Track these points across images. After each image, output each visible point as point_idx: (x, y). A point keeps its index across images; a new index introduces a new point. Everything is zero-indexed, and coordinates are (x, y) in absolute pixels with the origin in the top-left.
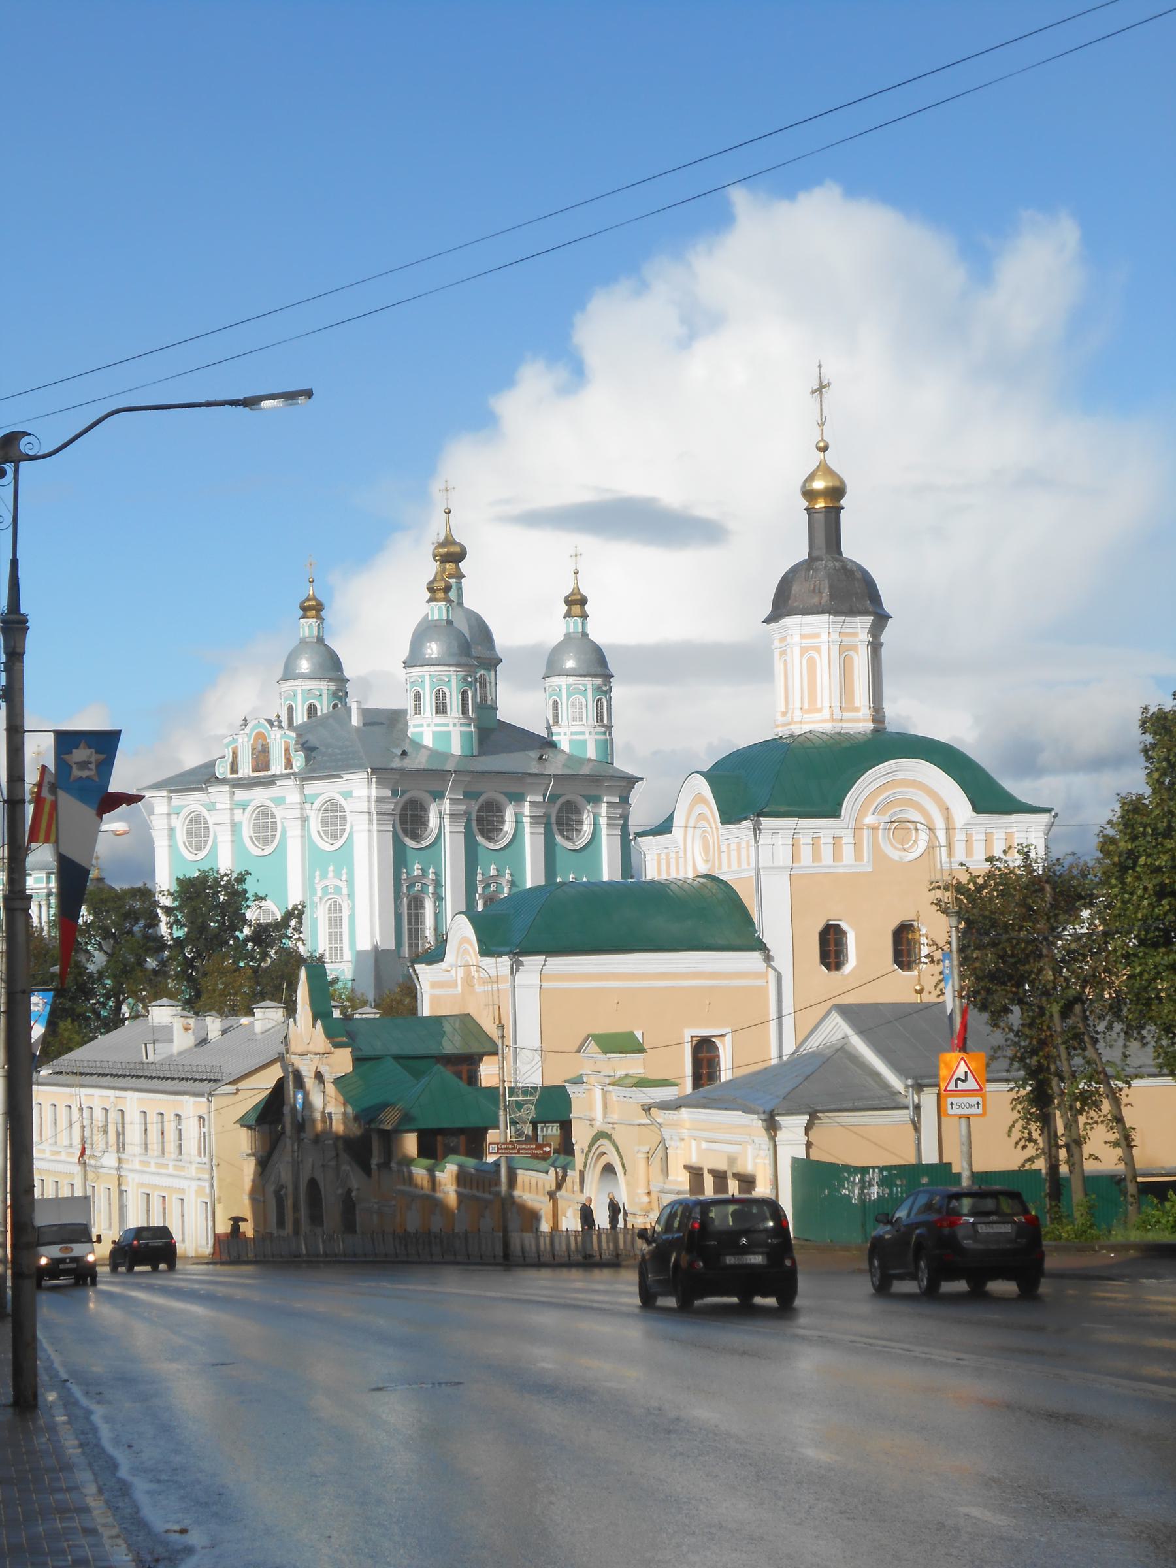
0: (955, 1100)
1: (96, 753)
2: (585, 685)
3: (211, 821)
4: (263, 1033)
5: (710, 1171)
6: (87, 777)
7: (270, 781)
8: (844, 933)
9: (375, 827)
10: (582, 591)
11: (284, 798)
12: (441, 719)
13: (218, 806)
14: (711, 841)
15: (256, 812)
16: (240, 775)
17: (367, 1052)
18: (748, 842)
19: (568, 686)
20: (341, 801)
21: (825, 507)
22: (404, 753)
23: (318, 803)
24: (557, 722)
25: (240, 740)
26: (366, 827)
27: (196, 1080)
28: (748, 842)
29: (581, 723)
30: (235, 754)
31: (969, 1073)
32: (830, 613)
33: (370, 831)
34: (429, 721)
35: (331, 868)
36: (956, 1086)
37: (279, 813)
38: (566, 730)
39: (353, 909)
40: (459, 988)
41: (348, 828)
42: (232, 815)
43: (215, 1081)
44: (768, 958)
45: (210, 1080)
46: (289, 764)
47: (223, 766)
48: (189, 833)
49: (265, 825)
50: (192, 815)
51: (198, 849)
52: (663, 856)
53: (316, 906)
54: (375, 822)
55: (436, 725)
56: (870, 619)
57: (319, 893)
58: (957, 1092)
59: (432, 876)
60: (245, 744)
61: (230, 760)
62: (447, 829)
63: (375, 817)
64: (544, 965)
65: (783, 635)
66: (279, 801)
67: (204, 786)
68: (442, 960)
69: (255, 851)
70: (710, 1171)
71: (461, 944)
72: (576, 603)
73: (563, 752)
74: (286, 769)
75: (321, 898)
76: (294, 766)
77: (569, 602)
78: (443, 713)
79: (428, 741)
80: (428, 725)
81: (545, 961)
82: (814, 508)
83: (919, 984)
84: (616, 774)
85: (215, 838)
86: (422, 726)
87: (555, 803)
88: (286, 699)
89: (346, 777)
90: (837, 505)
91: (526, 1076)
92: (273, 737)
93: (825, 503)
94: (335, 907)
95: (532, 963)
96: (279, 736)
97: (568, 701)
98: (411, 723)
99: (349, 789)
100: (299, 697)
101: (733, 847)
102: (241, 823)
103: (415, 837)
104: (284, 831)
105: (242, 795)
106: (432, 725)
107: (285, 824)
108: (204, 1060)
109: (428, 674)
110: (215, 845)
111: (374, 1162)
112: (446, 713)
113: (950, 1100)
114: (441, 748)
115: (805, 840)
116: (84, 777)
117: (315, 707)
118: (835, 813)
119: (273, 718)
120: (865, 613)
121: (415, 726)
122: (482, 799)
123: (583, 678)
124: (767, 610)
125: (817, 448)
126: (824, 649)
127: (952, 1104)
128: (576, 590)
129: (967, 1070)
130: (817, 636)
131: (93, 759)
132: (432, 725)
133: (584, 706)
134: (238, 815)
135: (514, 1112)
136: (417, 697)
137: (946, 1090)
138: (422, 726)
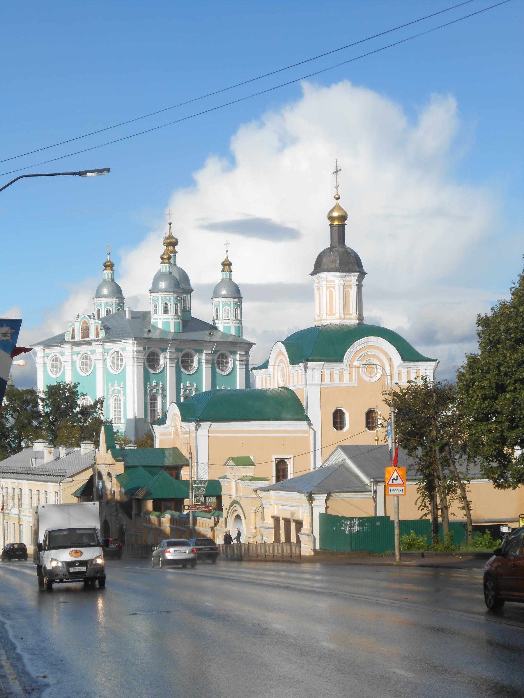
0: (392, 488)
1: (11, 329)
2: (230, 302)
3: (62, 360)
4: (84, 455)
5: (283, 519)
6: (7, 340)
7: (89, 343)
8: (344, 414)
9: (136, 364)
10: (230, 260)
11: (95, 350)
12: (166, 316)
13: (66, 354)
14: (285, 374)
15: (82, 357)
16: (76, 340)
17: (131, 464)
18: (302, 373)
19: (223, 302)
20: (121, 352)
21: (338, 224)
22: (149, 331)
24: (218, 318)
25: (76, 324)
26: (132, 364)
27: (54, 476)
28: (302, 373)
29: (228, 319)
30: (73, 330)
31: (398, 476)
32: (340, 271)
33: (133, 365)
34: (160, 317)
35: (116, 382)
36: (393, 482)
37: (93, 357)
38: (221, 321)
39: (125, 400)
40: (172, 436)
41: (124, 364)
42: (72, 357)
43: (63, 476)
44: (310, 424)
45: (61, 476)
46: (98, 335)
47: (68, 336)
48: (53, 365)
49: (87, 362)
50: (54, 357)
51: (57, 373)
52: (264, 378)
54: (136, 361)
55: (164, 319)
56: (357, 274)
57: (111, 393)
58: (393, 485)
59: (161, 386)
60: (78, 326)
61: (71, 333)
62: (168, 365)
63: (136, 359)
64: (210, 426)
65: (319, 281)
66: (93, 352)
67: (59, 344)
68: (165, 424)
69: (82, 374)
70: (283, 519)
71: (173, 416)
72: (227, 265)
73: (220, 331)
74: (96, 337)
75: (111, 395)
76: (100, 336)
77: (224, 265)
78: (167, 313)
79: (160, 326)
80: (160, 319)
81: (211, 424)
82: (333, 224)
83: (377, 436)
84: (243, 342)
85: (64, 367)
86: (157, 319)
87: (216, 354)
88: (97, 306)
89: (123, 341)
90: (343, 223)
91: (201, 475)
92: (91, 323)
93: (338, 222)
94: (118, 399)
95: (205, 425)
96: (93, 323)
97: (222, 309)
98: (152, 318)
99: (124, 347)
100: (103, 305)
101: (295, 374)
102: (76, 361)
103: (154, 368)
104: (95, 365)
105: (76, 348)
106: (162, 319)
107: (96, 362)
108: (58, 467)
109: (160, 296)
110: (64, 371)
111: (133, 513)
112: (168, 313)
113: (390, 488)
114: (166, 329)
115: (327, 372)
116: (5, 340)
117: (110, 310)
118: (341, 360)
119: (91, 314)
120: (355, 271)
121: (154, 319)
122: (184, 352)
123: (229, 299)
124: (312, 269)
125: (335, 198)
126: (337, 287)
127: (391, 490)
128: (227, 260)
129: (397, 475)
130: (334, 281)
131: (9, 332)
132: (162, 319)
133: (230, 311)
134: (75, 358)
135: (196, 492)
136: (155, 306)
137: (388, 484)
138: (157, 319)
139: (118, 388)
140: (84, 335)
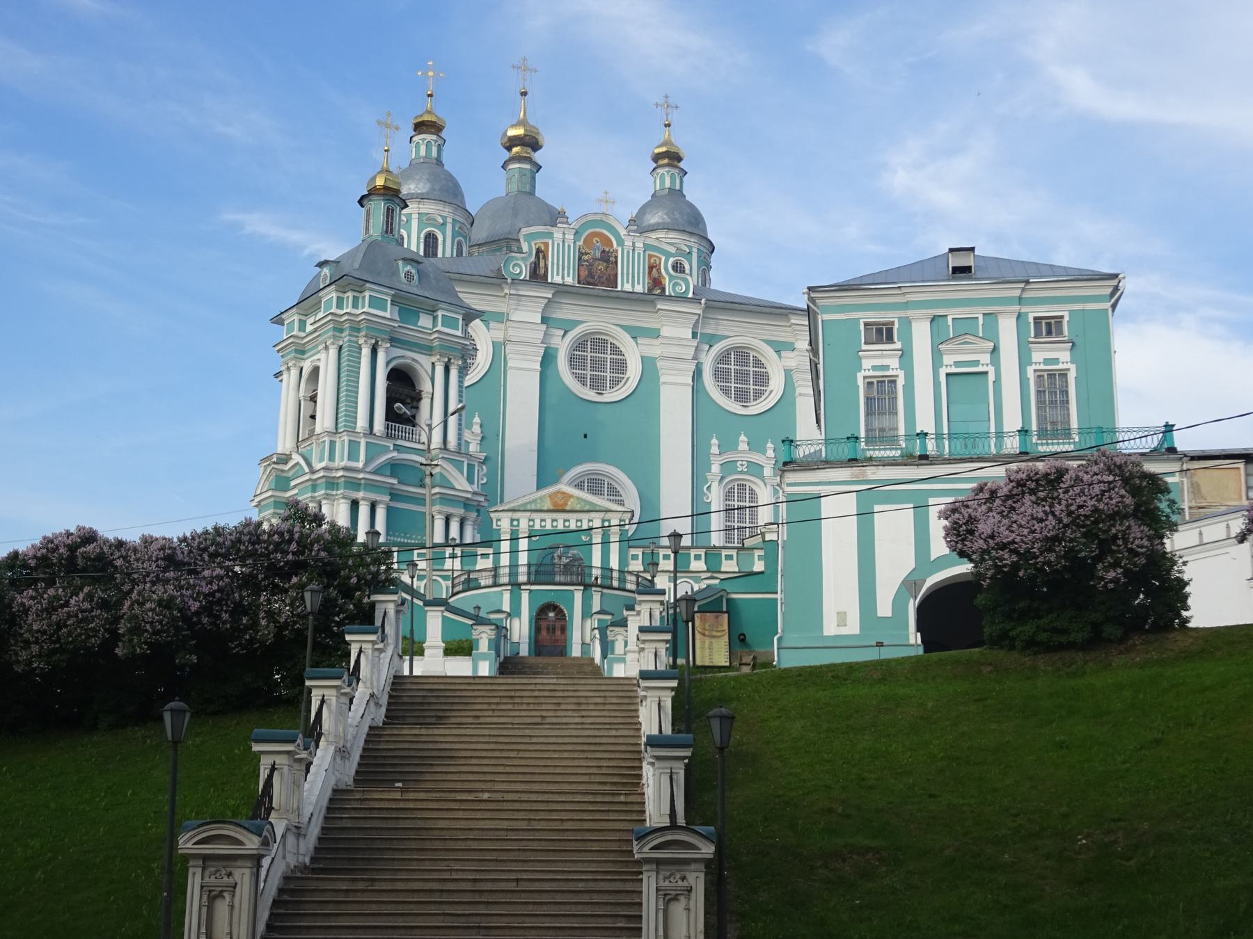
23: (718, 348)
25: (558, 235)
53: (709, 488)
57: (715, 468)
61: (533, 259)
92: (628, 243)
139: (756, 458)
140: (591, 275)
